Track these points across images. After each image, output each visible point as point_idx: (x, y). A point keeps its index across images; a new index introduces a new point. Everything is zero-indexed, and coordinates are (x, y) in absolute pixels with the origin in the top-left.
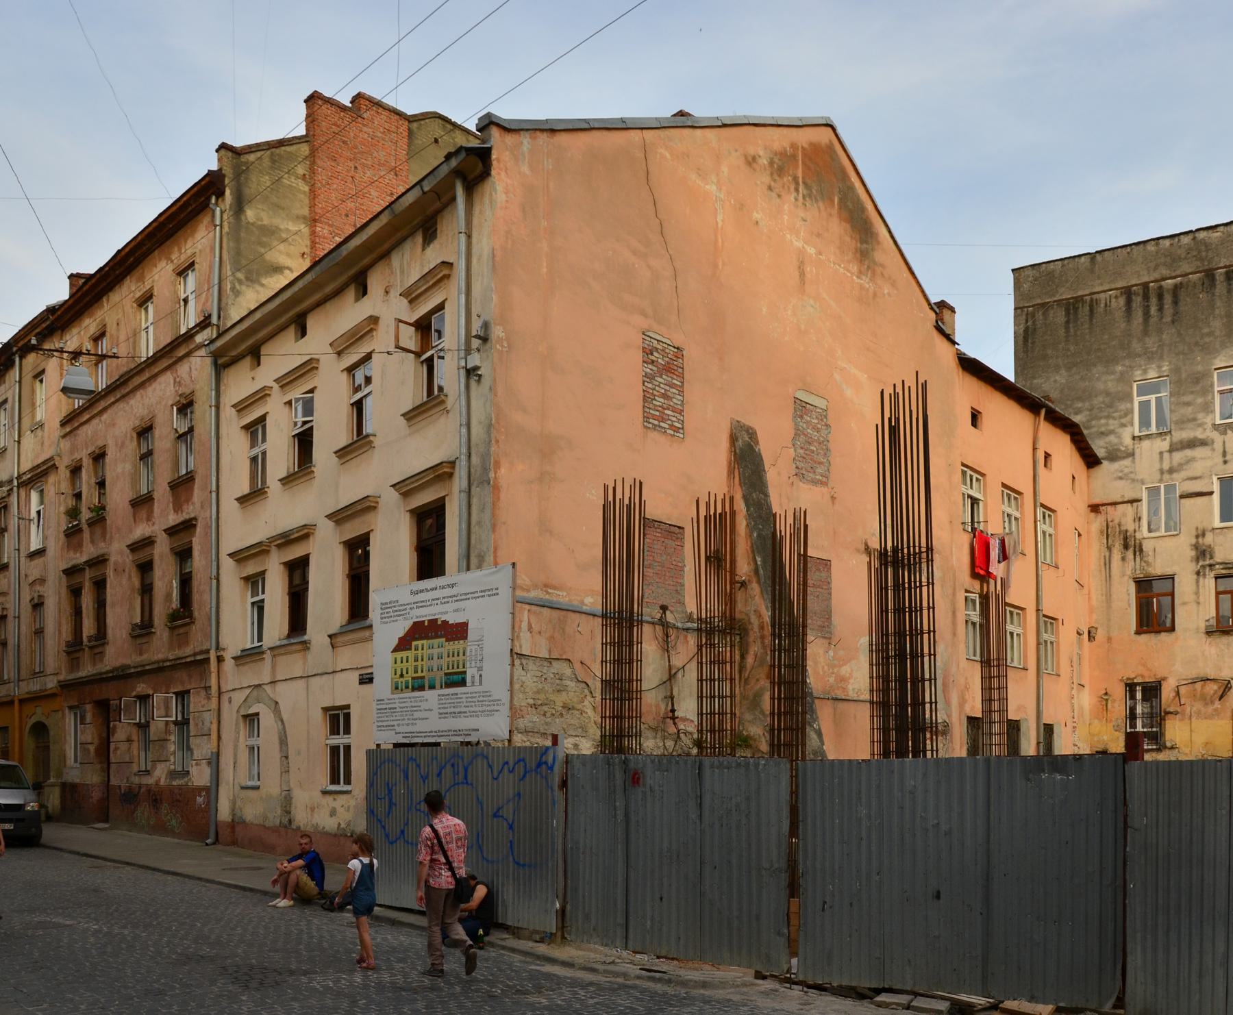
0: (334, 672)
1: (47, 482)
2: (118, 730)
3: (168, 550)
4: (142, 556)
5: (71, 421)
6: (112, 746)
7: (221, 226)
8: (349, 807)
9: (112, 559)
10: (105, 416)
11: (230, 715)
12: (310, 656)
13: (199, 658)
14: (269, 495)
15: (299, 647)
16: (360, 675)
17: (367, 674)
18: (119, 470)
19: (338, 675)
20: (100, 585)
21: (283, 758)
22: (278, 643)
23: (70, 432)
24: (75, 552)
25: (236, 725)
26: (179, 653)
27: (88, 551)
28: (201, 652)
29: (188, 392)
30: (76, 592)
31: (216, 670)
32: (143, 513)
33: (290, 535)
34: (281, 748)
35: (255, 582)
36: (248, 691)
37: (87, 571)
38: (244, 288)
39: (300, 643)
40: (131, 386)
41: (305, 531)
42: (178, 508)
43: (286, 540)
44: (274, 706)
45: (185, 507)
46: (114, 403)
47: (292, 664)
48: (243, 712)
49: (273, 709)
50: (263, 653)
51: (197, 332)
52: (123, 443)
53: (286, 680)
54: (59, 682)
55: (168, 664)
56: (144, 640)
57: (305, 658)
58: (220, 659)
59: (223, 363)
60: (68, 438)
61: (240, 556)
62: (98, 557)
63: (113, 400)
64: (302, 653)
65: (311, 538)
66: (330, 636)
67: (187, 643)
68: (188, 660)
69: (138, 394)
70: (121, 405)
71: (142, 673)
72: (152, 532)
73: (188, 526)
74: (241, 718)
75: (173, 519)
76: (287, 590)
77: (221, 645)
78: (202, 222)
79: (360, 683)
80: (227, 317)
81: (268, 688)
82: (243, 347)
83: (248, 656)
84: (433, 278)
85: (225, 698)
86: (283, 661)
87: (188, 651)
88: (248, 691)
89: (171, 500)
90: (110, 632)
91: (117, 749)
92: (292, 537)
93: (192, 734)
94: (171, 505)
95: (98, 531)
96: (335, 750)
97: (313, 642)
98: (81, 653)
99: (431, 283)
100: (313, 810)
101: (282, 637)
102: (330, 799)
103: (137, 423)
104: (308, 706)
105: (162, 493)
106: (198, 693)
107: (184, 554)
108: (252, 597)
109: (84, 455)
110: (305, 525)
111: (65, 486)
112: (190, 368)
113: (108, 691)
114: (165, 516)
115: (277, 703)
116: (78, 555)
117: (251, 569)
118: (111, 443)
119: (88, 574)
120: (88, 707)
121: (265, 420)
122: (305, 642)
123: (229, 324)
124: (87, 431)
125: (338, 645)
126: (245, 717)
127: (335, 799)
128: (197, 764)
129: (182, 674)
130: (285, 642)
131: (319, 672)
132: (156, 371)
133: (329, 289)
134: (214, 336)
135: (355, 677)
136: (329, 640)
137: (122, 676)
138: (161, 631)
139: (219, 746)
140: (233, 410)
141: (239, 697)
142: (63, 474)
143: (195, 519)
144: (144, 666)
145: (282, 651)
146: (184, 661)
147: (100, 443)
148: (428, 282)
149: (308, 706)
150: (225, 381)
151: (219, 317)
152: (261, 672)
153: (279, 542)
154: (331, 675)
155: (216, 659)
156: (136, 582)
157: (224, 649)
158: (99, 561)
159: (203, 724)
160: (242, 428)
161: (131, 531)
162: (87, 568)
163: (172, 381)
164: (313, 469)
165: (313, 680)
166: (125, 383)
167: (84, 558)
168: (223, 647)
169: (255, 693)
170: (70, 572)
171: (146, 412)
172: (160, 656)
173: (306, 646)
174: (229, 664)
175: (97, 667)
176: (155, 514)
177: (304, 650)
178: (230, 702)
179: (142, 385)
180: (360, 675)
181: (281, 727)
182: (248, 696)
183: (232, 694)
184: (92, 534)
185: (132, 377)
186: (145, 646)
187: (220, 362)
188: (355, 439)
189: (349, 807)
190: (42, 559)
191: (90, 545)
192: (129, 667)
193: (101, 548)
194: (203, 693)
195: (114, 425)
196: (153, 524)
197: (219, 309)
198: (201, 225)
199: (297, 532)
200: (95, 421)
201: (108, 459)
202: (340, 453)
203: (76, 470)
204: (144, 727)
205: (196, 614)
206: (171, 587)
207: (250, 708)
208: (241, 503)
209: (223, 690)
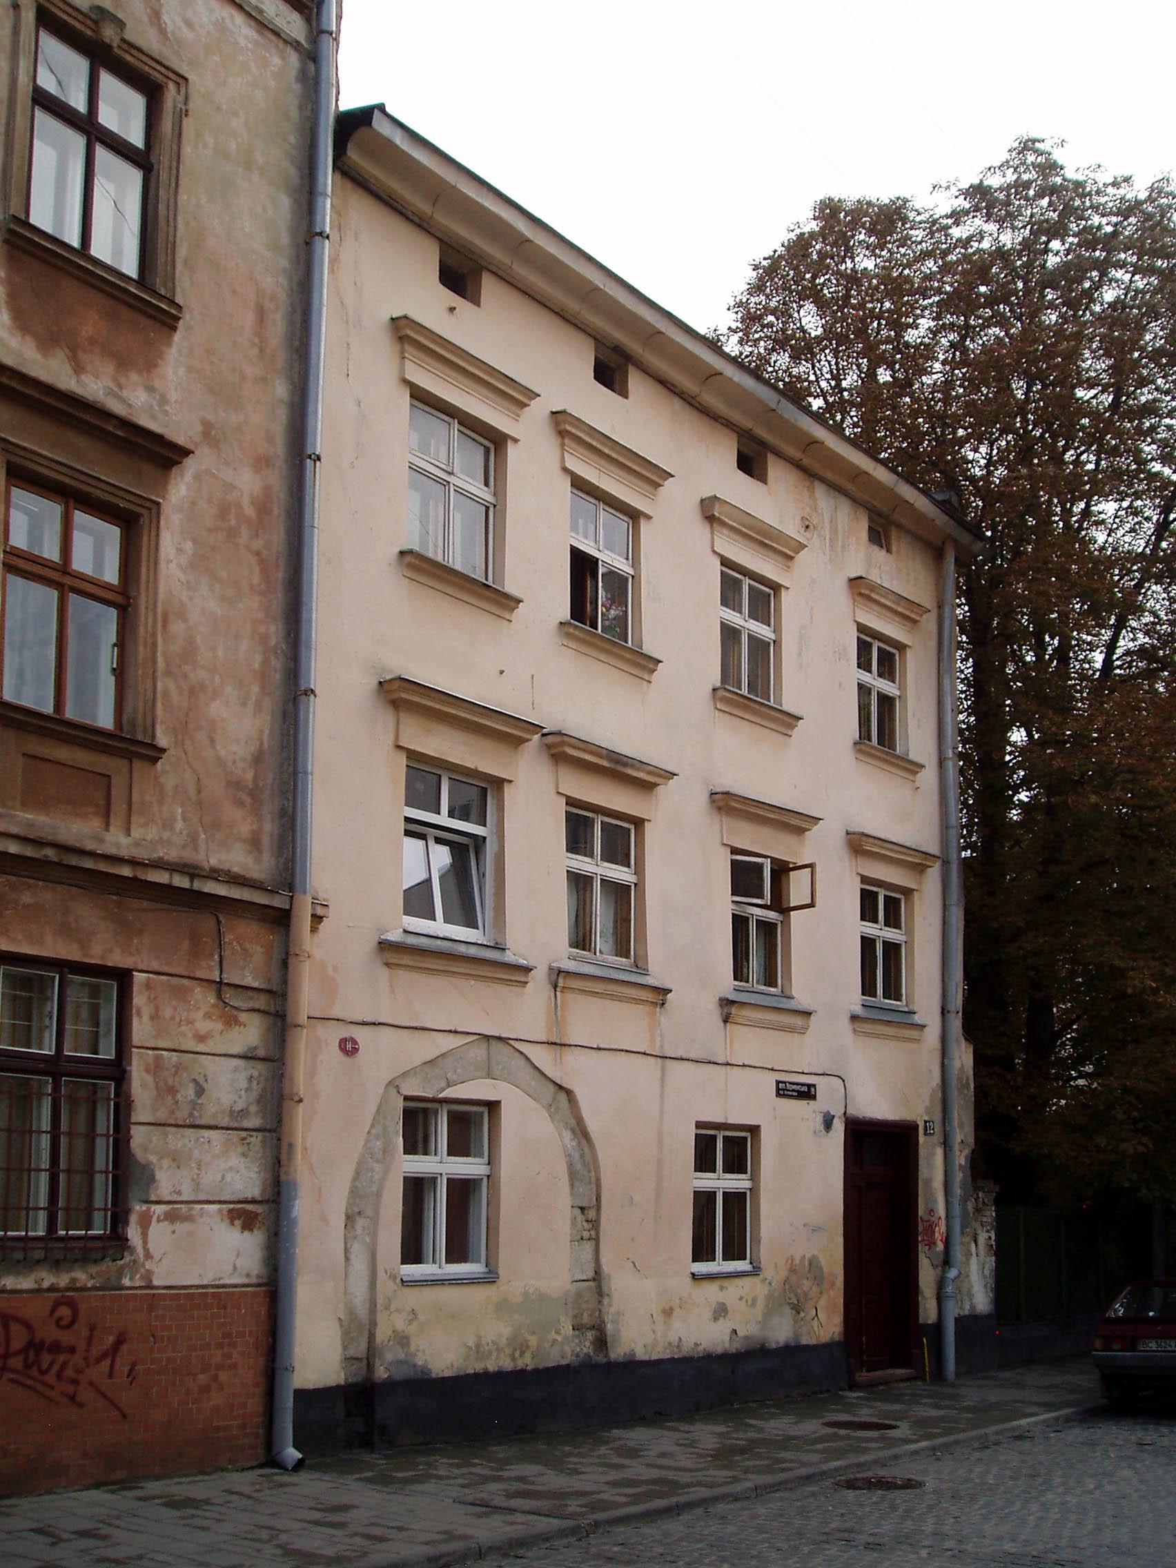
8: (754, 1300)
12: (665, 1020)
16: (778, 1082)
17: (790, 1083)
34: (572, 1186)
64: (647, 1008)
79: (778, 1095)
88: (448, 1043)
92: (629, 771)
99: (900, 609)
100: (668, 1312)
102: (711, 1289)
125: (740, 1020)
127: (722, 1288)
131: (693, 1055)
148: (899, 605)
159: (200, 1091)
165: (674, 1067)
180: (778, 1082)
183: (361, 1034)
189: (754, 1300)
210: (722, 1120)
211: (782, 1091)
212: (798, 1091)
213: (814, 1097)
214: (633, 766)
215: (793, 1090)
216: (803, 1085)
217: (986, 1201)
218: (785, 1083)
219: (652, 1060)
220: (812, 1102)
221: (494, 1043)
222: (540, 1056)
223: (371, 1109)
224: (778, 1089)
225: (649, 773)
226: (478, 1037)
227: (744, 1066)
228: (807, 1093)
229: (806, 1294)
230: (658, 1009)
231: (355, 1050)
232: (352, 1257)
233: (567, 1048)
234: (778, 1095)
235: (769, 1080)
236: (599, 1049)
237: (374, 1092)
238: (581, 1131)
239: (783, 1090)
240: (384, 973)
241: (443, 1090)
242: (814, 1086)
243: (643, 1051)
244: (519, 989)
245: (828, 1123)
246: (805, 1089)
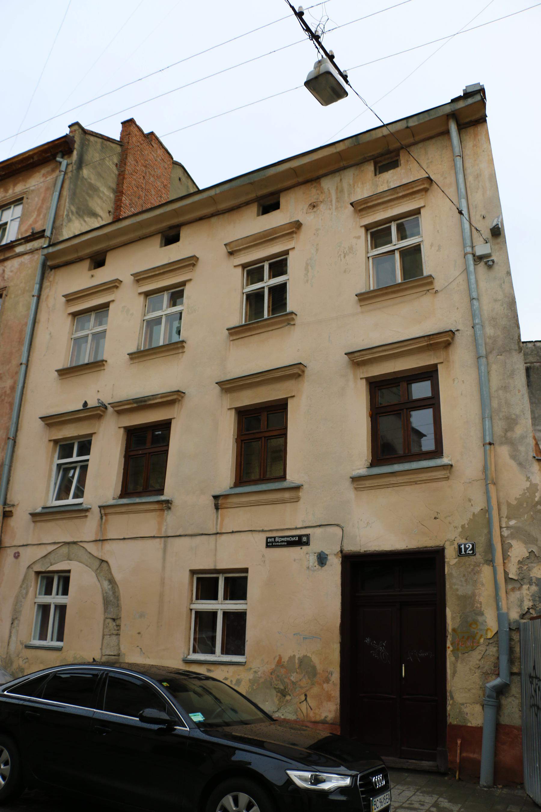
0: (217, 533)
7: (65, 173)
12: (170, 518)
14: (105, 368)
15: (156, 506)
19: (224, 537)
22: (112, 502)
25: (23, 581)
38: (74, 218)
39: (158, 502)
44: (96, 564)
48: (38, 568)
49: (95, 568)
51: (20, 244)
53: (124, 539)
64: (158, 513)
65: (177, 405)
74: (33, 575)
76: (123, 455)
78: (39, 172)
79: (267, 546)
80: (61, 234)
81: (91, 548)
82: (88, 251)
84: (404, 191)
97: (177, 502)
101: (116, 497)
104: (164, 567)
112: (4, 271)
121: (109, 307)
123: (61, 239)
126: (38, 573)
131: (190, 532)
133: (223, 206)
134: (45, 246)
140: (64, 299)
149: (164, 567)
150: (51, 279)
151: (52, 233)
154: (213, 538)
157: (13, 505)
160: (69, 314)
164: (184, 344)
168: (12, 503)
169: (65, 550)
177: (162, 510)
180: (267, 538)
182: (50, 553)
183: (21, 550)
187: (49, 263)
188: (243, 323)
197: (53, 228)
198: (38, 174)
202: (233, 331)
207: (51, 565)
208: (60, 375)
210: (212, 567)
211: (271, 544)
212: (287, 542)
213: (307, 543)
214: (150, 400)
215: (283, 542)
216: (293, 536)
218: (275, 538)
219: (158, 540)
220: (304, 548)
221: (71, 545)
222: (91, 548)
223: (21, 577)
224: (267, 542)
225: (161, 398)
226: (63, 544)
227: (233, 532)
230: (166, 512)
231: (19, 556)
232: (12, 635)
233: (105, 541)
234: (267, 546)
235: (261, 539)
236: (124, 539)
237: (23, 570)
239: (272, 542)
240: (32, 525)
241: (49, 567)
242: (308, 536)
243: (153, 535)
244: (84, 519)
245: (322, 559)
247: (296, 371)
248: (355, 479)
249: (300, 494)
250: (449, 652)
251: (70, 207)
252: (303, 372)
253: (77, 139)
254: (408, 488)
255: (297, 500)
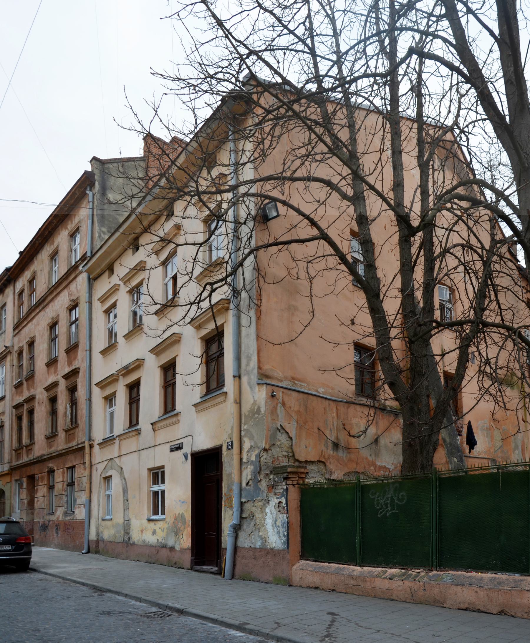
1: (6, 361)
2: (39, 491)
3: (65, 387)
4: (52, 393)
5: (18, 327)
6: (36, 500)
8: (164, 529)
9: (37, 397)
10: (34, 321)
11: (97, 478)
13: (80, 446)
15: (134, 433)
18: (41, 348)
19: (157, 447)
20: (31, 412)
21: (126, 501)
22: (123, 432)
23: (18, 333)
24: (19, 396)
26: (71, 445)
27: (26, 394)
28: (82, 443)
29: (75, 298)
30: (19, 418)
31: (89, 452)
32: (52, 369)
33: (129, 366)
35: (110, 399)
36: (106, 463)
37: (25, 404)
40: (47, 301)
41: (137, 363)
42: (70, 363)
43: (127, 370)
45: (73, 363)
46: (38, 313)
47: (130, 444)
48: (103, 476)
50: (114, 439)
52: (43, 334)
54: (10, 467)
55: (64, 451)
56: (52, 440)
57: (138, 439)
58: (91, 446)
59: (92, 280)
60: (17, 336)
61: (102, 385)
62: (29, 397)
63: (38, 311)
66: (152, 424)
67: (74, 439)
68: (74, 448)
69: (50, 305)
70: (42, 313)
71: (51, 458)
72: (57, 379)
73: (75, 372)
74: (102, 479)
75: (67, 370)
76: (128, 401)
77: (92, 439)
81: (117, 460)
83: (107, 442)
85: (94, 468)
86: (125, 443)
87: (74, 443)
88: (106, 463)
89: (66, 360)
90: (36, 437)
91: (38, 501)
92: (130, 368)
93: (76, 490)
94: (66, 363)
95: (30, 382)
96: (156, 493)
98: (21, 450)
103: (50, 321)
105: (62, 357)
106: (80, 467)
107: (72, 390)
108: (109, 408)
109: (24, 343)
110: (137, 359)
111: (15, 362)
113: (34, 470)
114: (64, 368)
115: (122, 468)
116: (21, 397)
117: (108, 391)
118: (37, 335)
119: (26, 407)
120: (25, 479)
122: (137, 430)
124: (26, 330)
125: (157, 429)
127: (155, 524)
128: (79, 507)
129: (71, 457)
130: (127, 431)
131: (146, 447)
132: (59, 290)
135: (167, 447)
136: (151, 426)
137: (41, 461)
138: (62, 435)
139: (90, 496)
141: (101, 467)
142: (15, 355)
143: (79, 368)
144: (52, 454)
145: (125, 437)
146: (72, 449)
147: (32, 336)
152: (113, 451)
153: (123, 372)
155: (89, 446)
156: (48, 407)
158: (31, 399)
161: (46, 381)
162: (25, 404)
163: (67, 294)
165: (142, 452)
166: (44, 300)
167: (24, 398)
169: (110, 464)
170: (17, 407)
171: (54, 314)
172: (60, 448)
173: (139, 431)
174: (96, 448)
175: (29, 457)
176: (58, 369)
178: (97, 470)
179: (52, 299)
181: (124, 482)
184: (28, 385)
185: (47, 297)
186: (52, 443)
189: (164, 529)
190: (4, 402)
191: (27, 391)
192: (44, 455)
193: (32, 392)
194: (82, 466)
195: (38, 325)
196: (58, 375)
199: (133, 364)
200: (30, 324)
201: (36, 344)
203: (20, 353)
204: (51, 488)
205: (79, 422)
206: (66, 408)
209: (93, 463)
217: (276, 479)
228: (179, 448)
229: (179, 528)
238: (125, 479)
242: (182, 443)
246: (178, 446)
247: (174, 338)
248: (195, 405)
249: (179, 418)
250: (223, 506)
251: (100, 230)
252: (180, 338)
253: (97, 172)
254: (213, 409)
255: (178, 422)
